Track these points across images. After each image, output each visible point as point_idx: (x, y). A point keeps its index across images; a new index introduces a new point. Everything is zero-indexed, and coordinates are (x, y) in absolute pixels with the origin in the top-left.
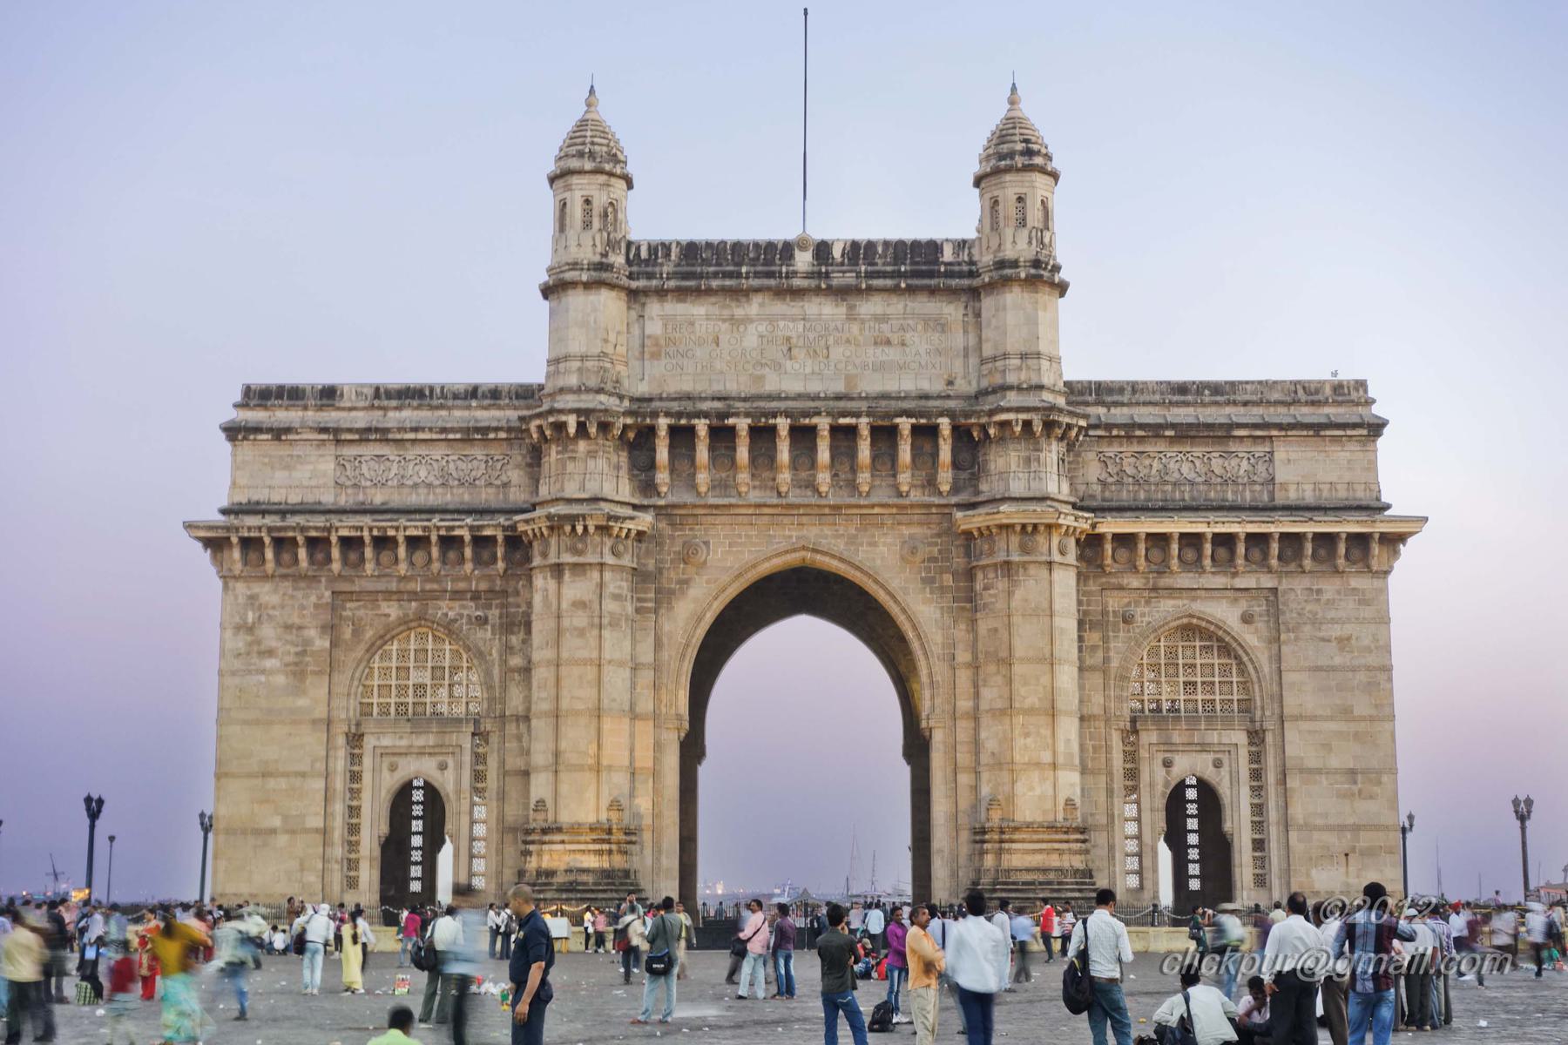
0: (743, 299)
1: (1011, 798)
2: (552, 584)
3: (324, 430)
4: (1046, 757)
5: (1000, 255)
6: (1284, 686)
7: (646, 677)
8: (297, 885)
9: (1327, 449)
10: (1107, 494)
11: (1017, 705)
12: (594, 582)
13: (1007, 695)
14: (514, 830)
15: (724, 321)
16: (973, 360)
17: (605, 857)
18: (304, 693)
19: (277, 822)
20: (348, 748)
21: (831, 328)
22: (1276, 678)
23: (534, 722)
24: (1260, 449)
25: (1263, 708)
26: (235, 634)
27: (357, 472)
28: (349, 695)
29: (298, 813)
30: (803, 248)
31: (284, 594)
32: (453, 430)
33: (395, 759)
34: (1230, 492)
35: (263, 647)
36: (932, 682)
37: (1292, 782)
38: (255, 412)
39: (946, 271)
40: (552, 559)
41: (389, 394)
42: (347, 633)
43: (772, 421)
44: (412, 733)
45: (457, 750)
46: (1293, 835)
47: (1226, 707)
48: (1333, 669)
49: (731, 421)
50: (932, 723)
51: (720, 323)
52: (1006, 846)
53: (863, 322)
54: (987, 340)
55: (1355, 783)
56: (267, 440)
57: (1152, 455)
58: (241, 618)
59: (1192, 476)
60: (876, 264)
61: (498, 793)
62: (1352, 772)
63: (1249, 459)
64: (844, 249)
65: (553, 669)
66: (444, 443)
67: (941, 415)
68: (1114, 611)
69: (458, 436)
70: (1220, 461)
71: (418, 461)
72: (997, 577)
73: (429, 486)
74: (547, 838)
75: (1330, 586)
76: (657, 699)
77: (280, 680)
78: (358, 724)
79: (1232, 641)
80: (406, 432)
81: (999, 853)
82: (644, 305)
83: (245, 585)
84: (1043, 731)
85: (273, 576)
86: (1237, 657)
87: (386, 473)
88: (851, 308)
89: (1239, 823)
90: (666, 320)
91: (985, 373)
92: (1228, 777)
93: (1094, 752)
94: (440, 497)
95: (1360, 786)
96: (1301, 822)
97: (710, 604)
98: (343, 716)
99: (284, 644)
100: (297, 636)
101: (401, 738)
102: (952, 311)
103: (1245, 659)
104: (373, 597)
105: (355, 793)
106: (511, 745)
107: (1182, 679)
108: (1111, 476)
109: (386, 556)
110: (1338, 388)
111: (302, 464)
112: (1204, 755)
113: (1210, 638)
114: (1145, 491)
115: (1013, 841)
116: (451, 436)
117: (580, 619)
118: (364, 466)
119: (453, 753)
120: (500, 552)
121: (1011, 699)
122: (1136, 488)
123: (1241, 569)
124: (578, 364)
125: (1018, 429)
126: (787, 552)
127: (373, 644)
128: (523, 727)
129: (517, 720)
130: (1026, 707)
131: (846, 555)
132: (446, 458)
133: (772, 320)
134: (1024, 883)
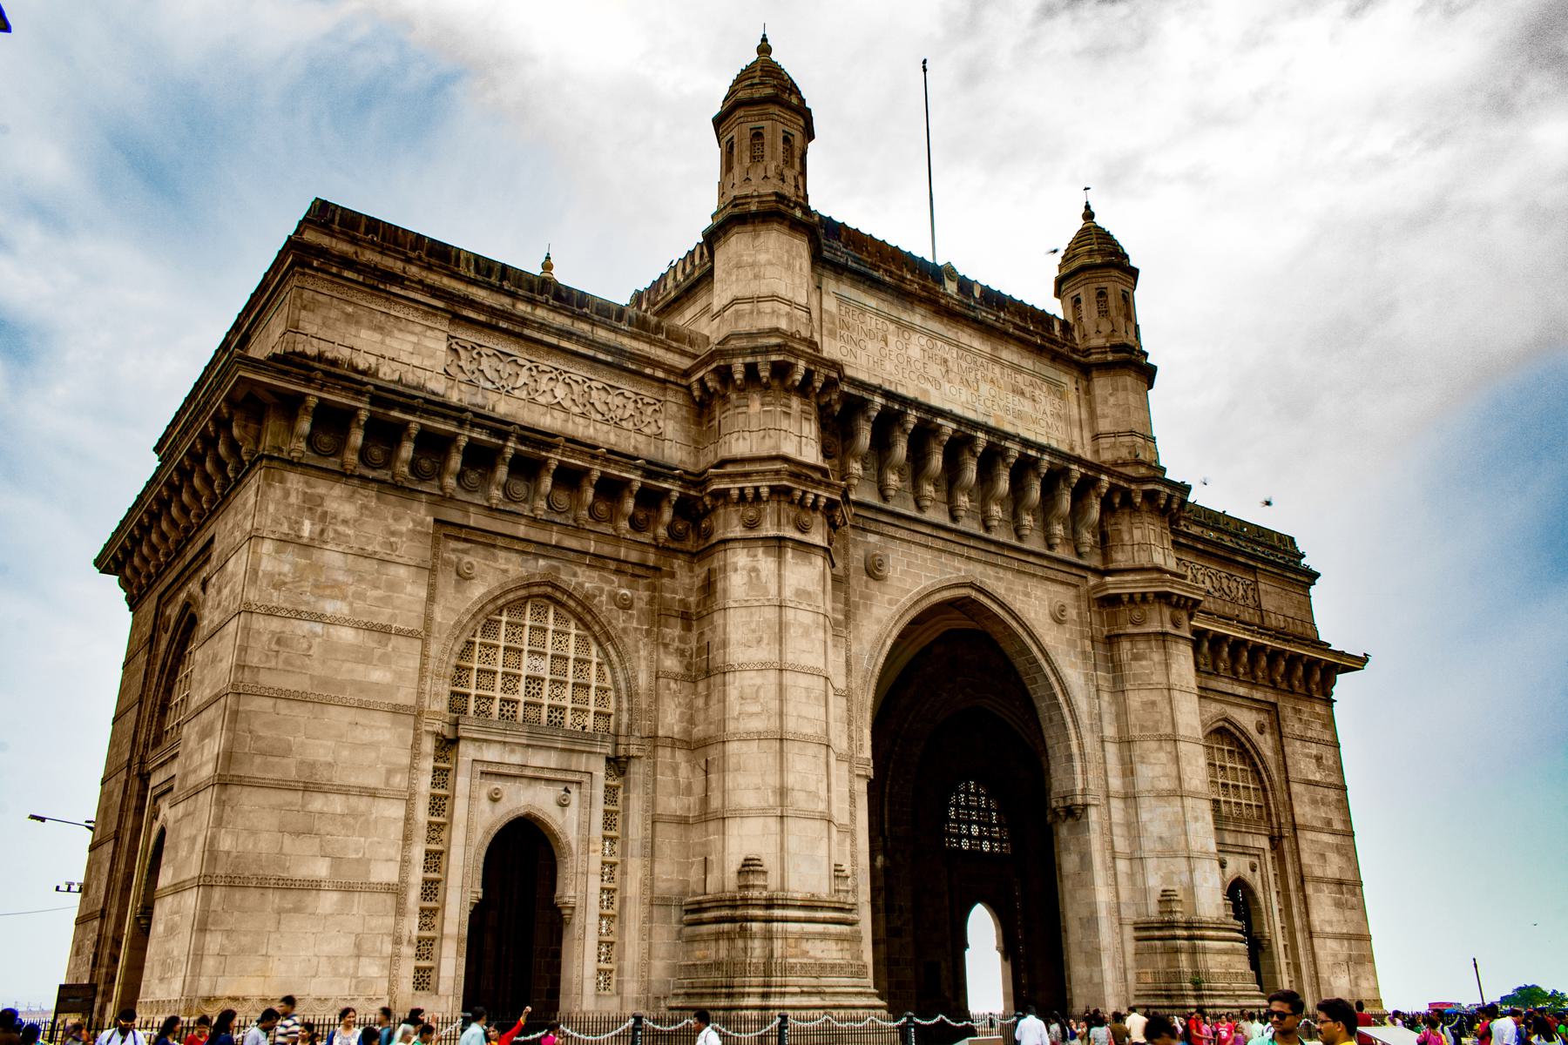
0: (909, 307)
1: (1191, 890)
2: (766, 564)
3: (435, 291)
5: (1116, 340)
6: (1293, 797)
8: (346, 982)
11: (1186, 786)
13: (1174, 773)
14: (665, 902)
15: (892, 321)
16: (1087, 435)
17: (846, 945)
18: (385, 660)
19: (321, 869)
21: (979, 364)
22: (1284, 787)
23: (732, 747)
24: (1250, 578)
27: (474, 366)
29: (360, 855)
31: (364, 507)
32: (607, 348)
33: (498, 784)
36: (1083, 754)
37: (1310, 889)
38: (334, 240)
40: (768, 529)
42: (446, 581)
43: (973, 433)
44: (528, 746)
45: (586, 778)
46: (1316, 941)
48: (1316, 784)
49: (939, 421)
50: (1090, 800)
51: (888, 322)
52: (1199, 943)
53: (1002, 364)
54: (1105, 416)
55: (1343, 893)
56: (356, 282)
58: (290, 528)
59: (1212, 590)
61: (644, 847)
64: (981, 292)
65: (772, 676)
66: (588, 363)
69: (609, 359)
71: (553, 376)
72: (1151, 648)
73: (565, 410)
74: (777, 913)
76: (850, 738)
77: (347, 635)
78: (455, 724)
79: (1251, 749)
80: (548, 333)
81: (1193, 952)
82: (821, 276)
83: (302, 478)
85: (351, 476)
86: (1255, 765)
87: (513, 379)
88: (994, 349)
90: (841, 299)
91: (1108, 446)
94: (581, 428)
96: (1318, 929)
97: (891, 631)
99: (358, 581)
100: (378, 571)
101: (512, 751)
102: (1068, 381)
103: (1260, 767)
104: (487, 541)
105: (436, 830)
106: (665, 778)
107: (1220, 781)
109: (520, 488)
110: (1281, 537)
111: (400, 330)
113: (1231, 744)
115: (1202, 938)
116: (601, 356)
118: (484, 360)
119: (579, 783)
120: (667, 515)
121: (1180, 779)
123: (1261, 681)
124: (787, 308)
125: (1163, 502)
126: (957, 586)
127: (481, 610)
128: (680, 756)
129: (673, 747)
131: (1008, 599)
132: (589, 383)
133: (932, 336)
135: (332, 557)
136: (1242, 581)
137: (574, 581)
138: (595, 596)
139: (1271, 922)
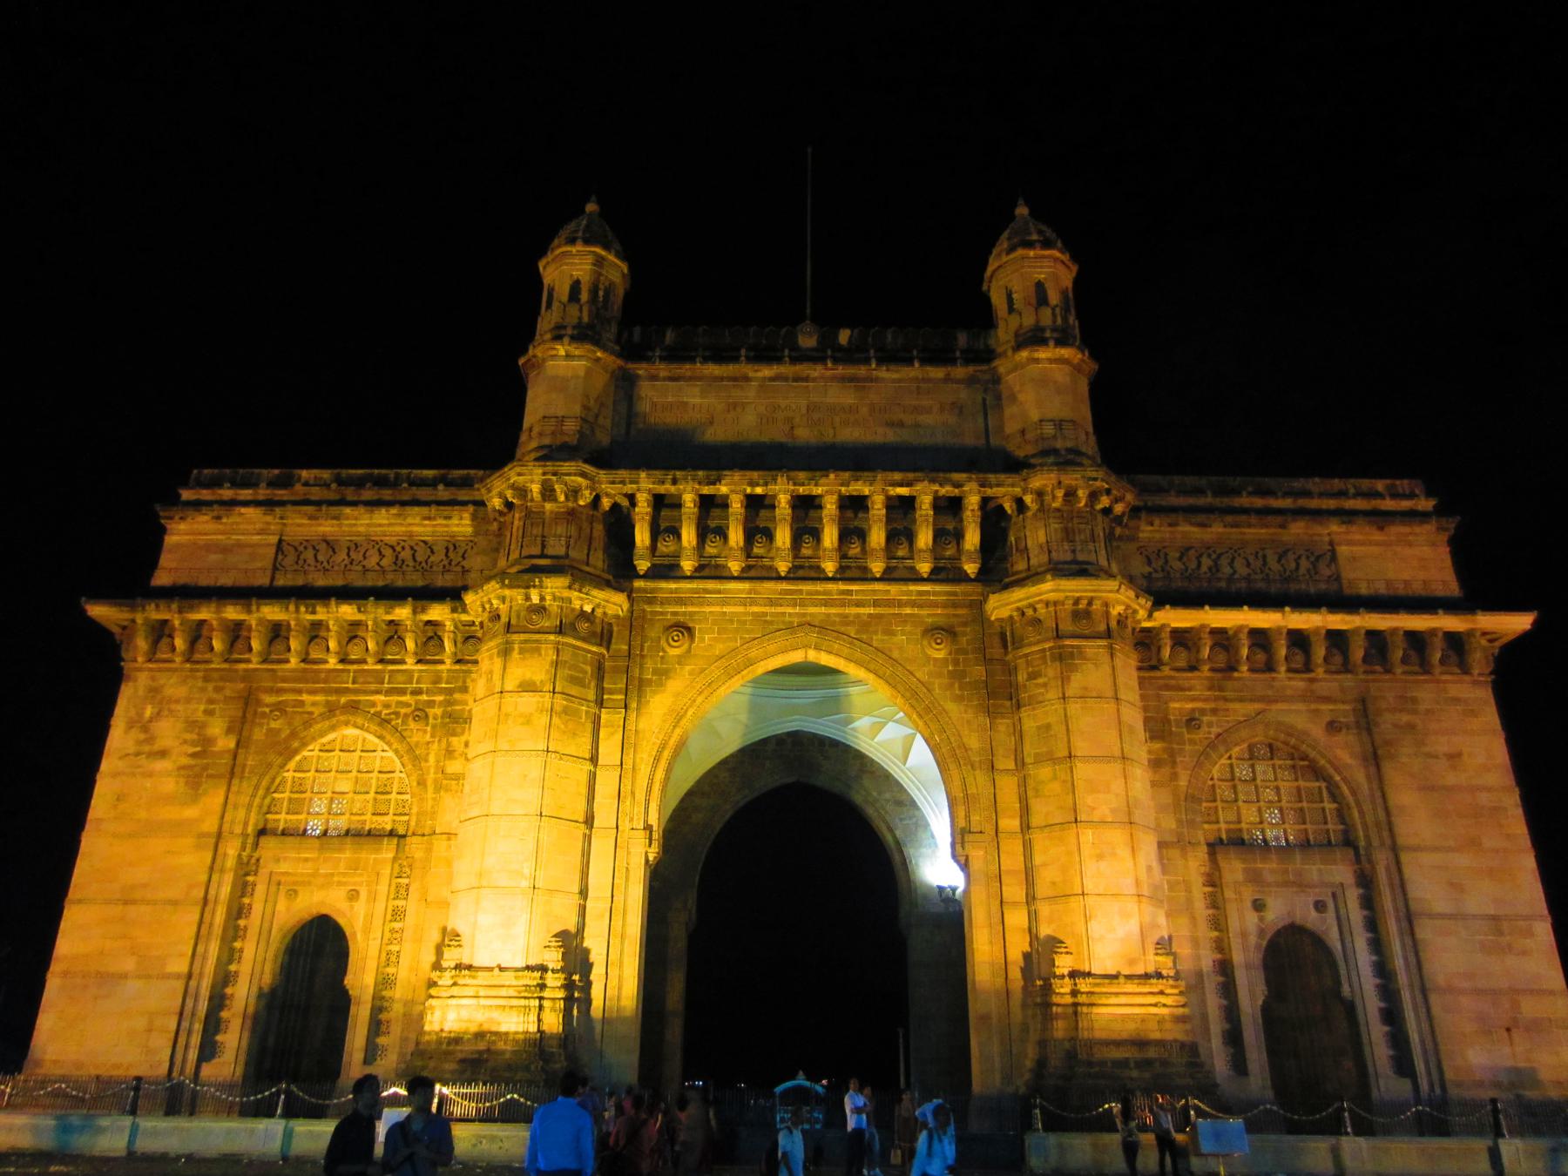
2: (498, 662)
11: (1082, 817)
19: (129, 964)
25: (1367, 837)
28: (250, 806)
35: (157, 747)
37: (1425, 931)
46: (1434, 999)
62: (1495, 918)
63: (1308, 558)
68: (1176, 720)
72: (1045, 663)
75: (1425, 694)
77: (170, 785)
86: (1328, 780)
92: (1335, 929)
98: (238, 830)
103: (1338, 778)
108: (1156, 571)
139: (1354, 978)
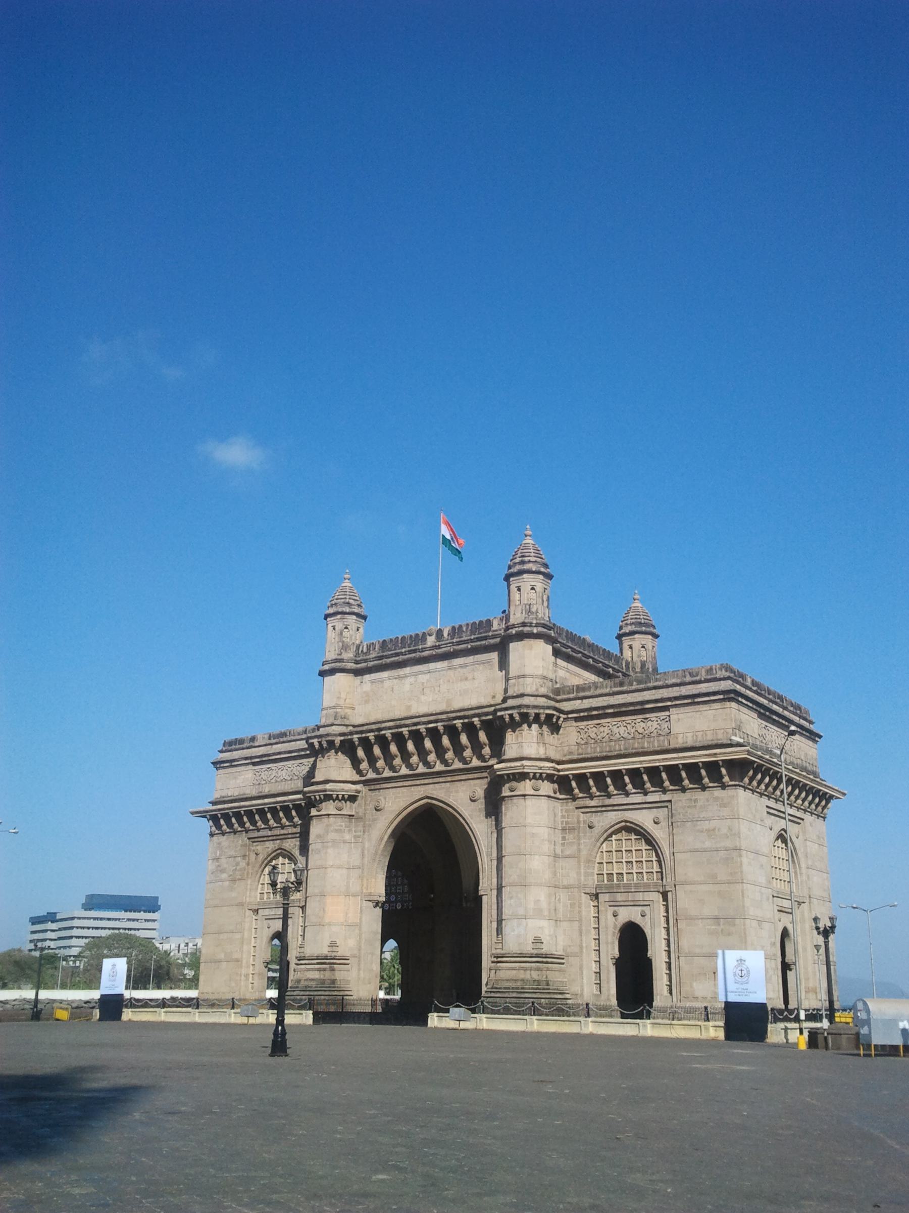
4: (521, 911)
7: (355, 873)
9: (701, 710)
10: (580, 751)
12: (325, 824)
15: (396, 678)
19: (222, 956)
20: (254, 916)
26: (213, 862)
30: (430, 635)
34: (646, 744)
39: (492, 635)
41: (275, 737)
47: (650, 877)
49: (383, 732)
51: (394, 680)
53: (455, 668)
57: (604, 725)
59: (626, 735)
60: (462, 637)
62: (717, 918)
67: (474, 717)
70: (642, 724)
75: (701, 796)
77: (227, 883)
84: (519, 895)
89: (657, 951)
90: (372, 682)
93: (571, 907)
95: (722, 927)
96: (687, 952)
111: (239, 776)
112: (636, 908)
114: (600, 747)
117: (319, 846)
122: (596, 745)
125: (507, 720)
130: (511, 881)
133: (416, 674)
134: (505, 988)
135: (223, 861)
136: (657, 719)
137: (288, 844)
138: (293, 848)
